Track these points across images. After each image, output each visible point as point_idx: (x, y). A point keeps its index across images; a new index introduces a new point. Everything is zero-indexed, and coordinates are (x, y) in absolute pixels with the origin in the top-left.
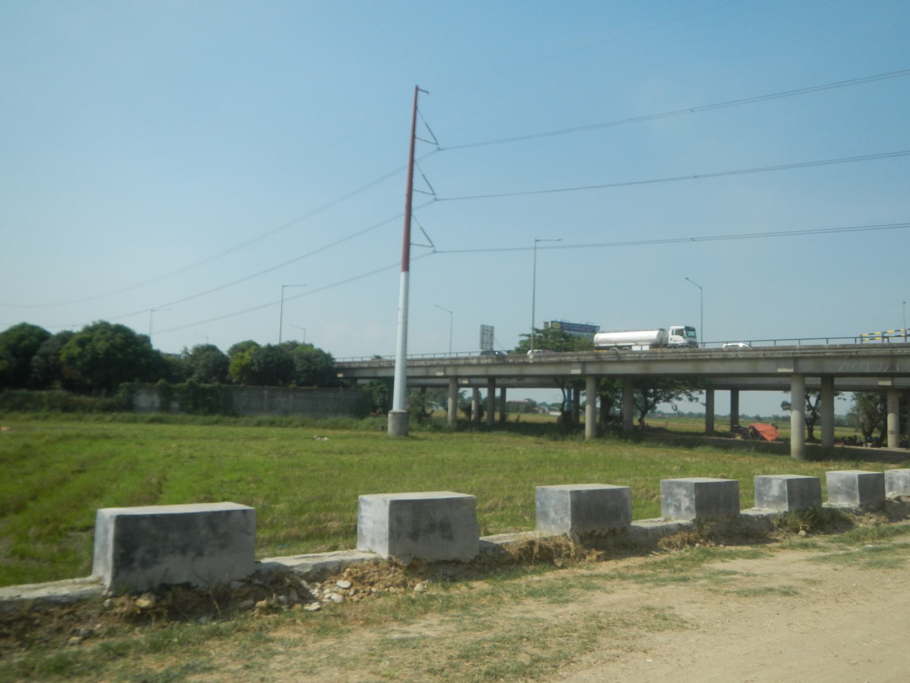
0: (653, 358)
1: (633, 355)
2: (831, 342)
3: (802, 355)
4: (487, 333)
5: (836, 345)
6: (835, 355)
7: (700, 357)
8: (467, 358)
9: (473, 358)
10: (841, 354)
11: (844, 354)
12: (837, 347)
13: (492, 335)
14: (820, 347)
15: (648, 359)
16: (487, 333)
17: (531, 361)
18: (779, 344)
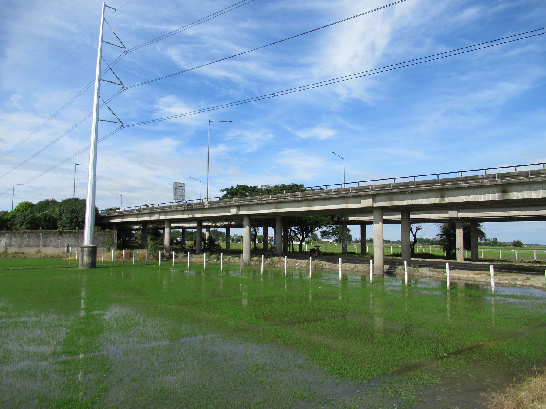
0: (279, 200)
1: (267, 199)
2: (397, 181)
3: (377, 192)
4: (179, 188)
5: (400, 183)
6: (400, 191)
7: (309, 198)
8: (170, 207)
9: (174, 206)
10: (404, 190)
11: (406, 190)
12: (401, 185)
13: (184, 190)
14: (388, 186)
15: (276, 201)
16: (179, 188)
17: (206, 207)
18: (361, 185)
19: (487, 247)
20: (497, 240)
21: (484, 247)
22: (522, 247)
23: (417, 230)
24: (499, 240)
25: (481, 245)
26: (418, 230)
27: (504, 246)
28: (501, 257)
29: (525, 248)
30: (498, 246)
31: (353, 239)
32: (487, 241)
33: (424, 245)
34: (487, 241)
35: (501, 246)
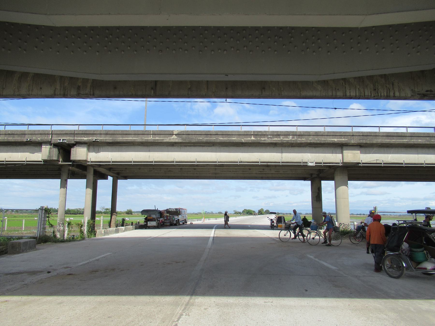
21: (104, 215)
22: (132, 214)
25: (101, 213)
27: (119, 214)
28: (7, 227)
29: (134, 215)
32: (108, 210)
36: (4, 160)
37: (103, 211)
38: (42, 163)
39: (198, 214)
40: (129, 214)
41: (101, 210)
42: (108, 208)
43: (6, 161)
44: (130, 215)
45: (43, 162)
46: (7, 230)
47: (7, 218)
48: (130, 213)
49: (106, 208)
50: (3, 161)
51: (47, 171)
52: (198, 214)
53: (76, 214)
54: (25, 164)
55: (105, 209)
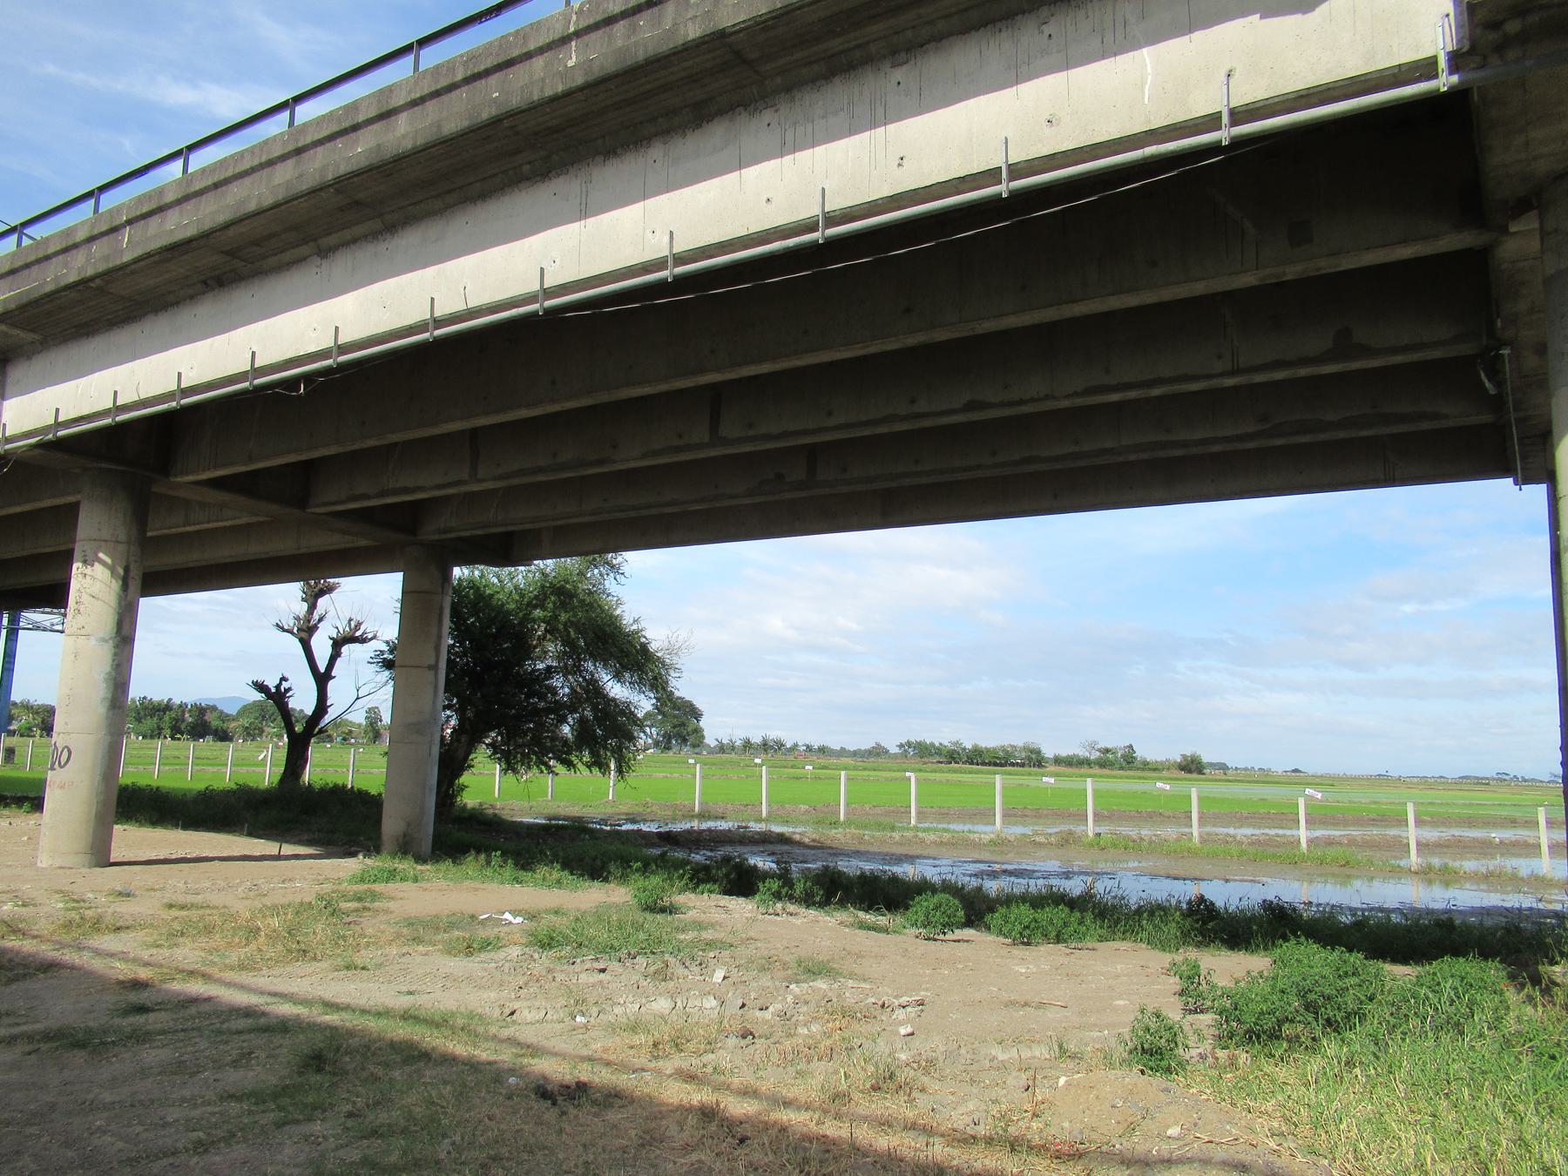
19: (1106, 771)
20: (1135, 752)
21: (1096, 770)
22: (1204, 774)
23: (338, 644)
24: (1142, 753)
25: (1089, 764)
26: (345, 649)
27: (1155, 770)
28: (846, 814)
29: (1210, 777)
30: (1138, 769)
31: (710, 740)
32: (1110, 756)
33: (925, 763)
34: (1110, 756)
35: (1143, 769)
36: (997, 161)
37: (1095, 755)
38: (1445, 81)
39: (1488, 784)
40: (1190, 771)
41: (1087, 754)
42: (1110, 746)
43: (1016, 171)
44: (1195, 776)
45: (1454, 67)
46: (848, 823)
47: (811, 768)
48: (1193, 767)
49: (1102, 745)
50: (992, 175)
51: (1234, 372)
52: (1488, 784)
53: (1001, 765)
54: (1214, 149)
55: (1099, 750)
